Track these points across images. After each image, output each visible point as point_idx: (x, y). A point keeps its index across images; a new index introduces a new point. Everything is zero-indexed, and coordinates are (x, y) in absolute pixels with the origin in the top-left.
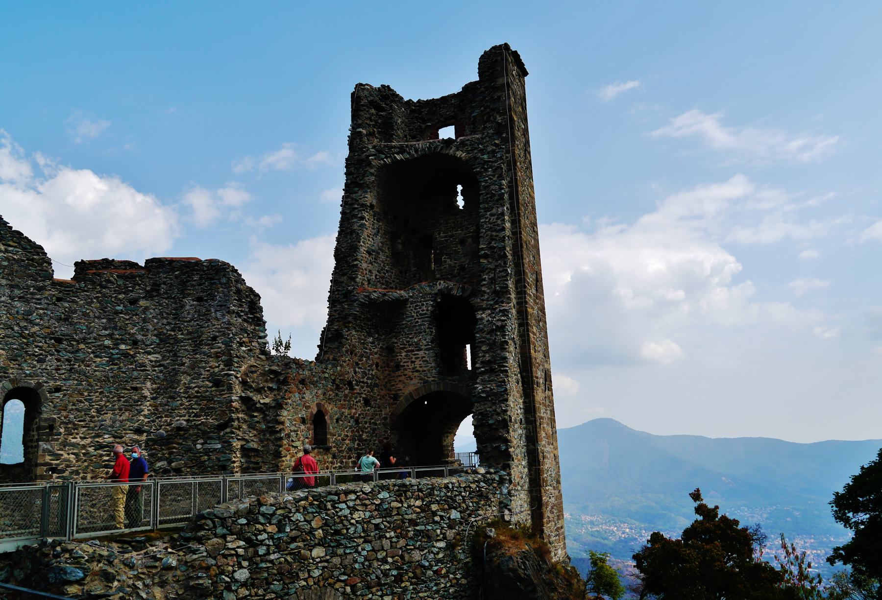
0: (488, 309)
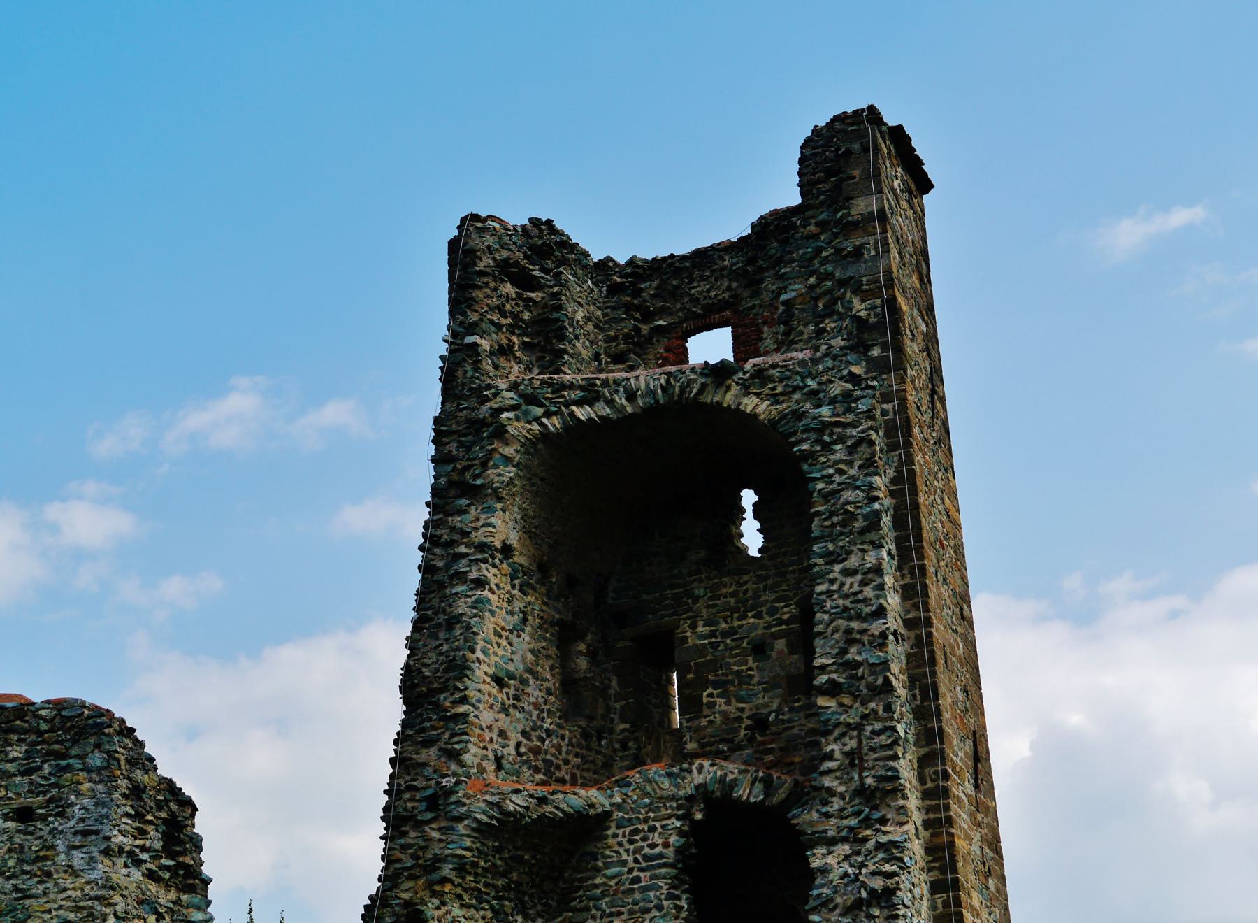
0: (844, 840)
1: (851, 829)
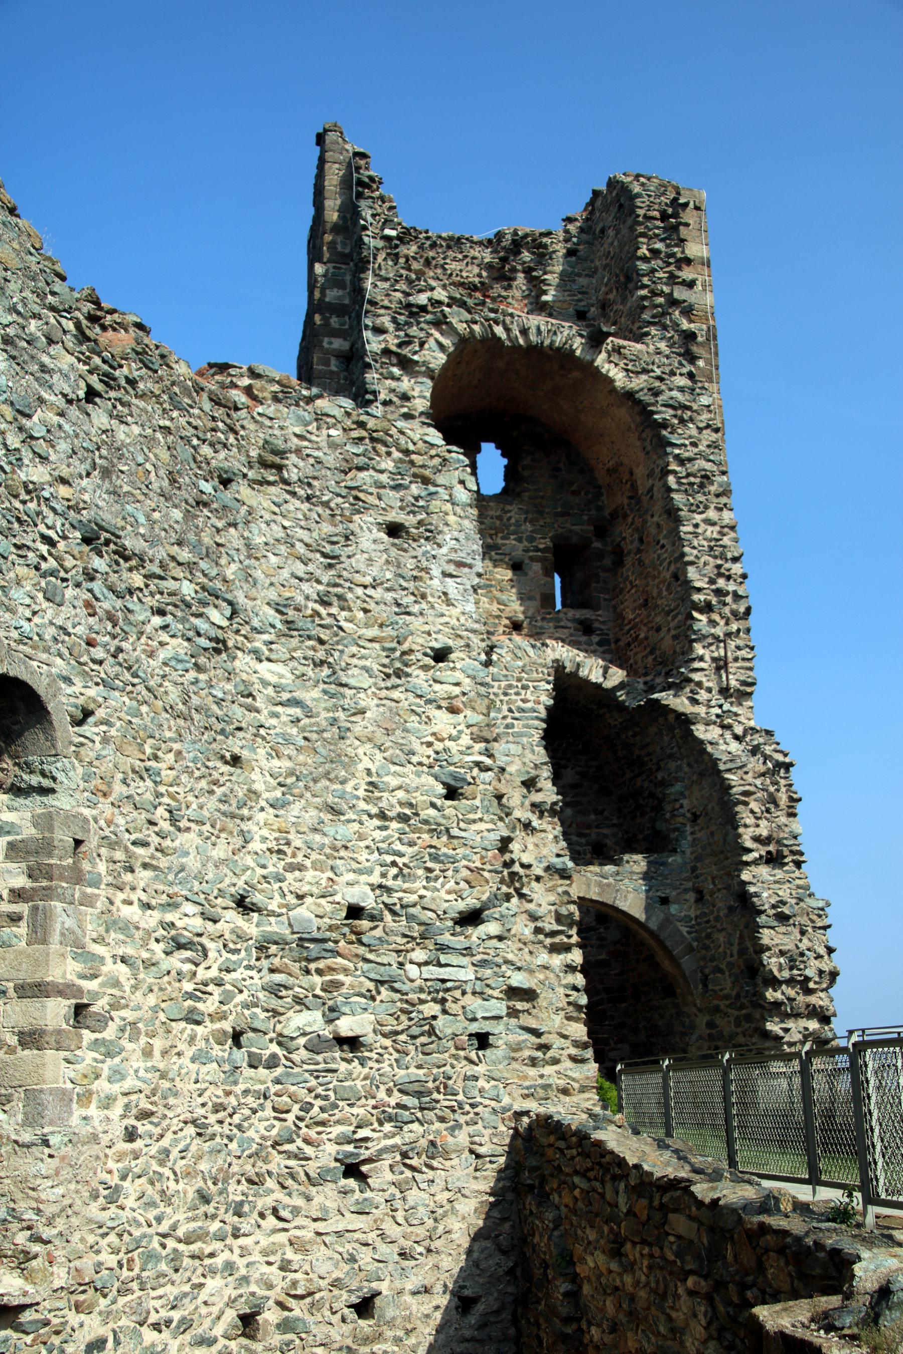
1: (718, 716)
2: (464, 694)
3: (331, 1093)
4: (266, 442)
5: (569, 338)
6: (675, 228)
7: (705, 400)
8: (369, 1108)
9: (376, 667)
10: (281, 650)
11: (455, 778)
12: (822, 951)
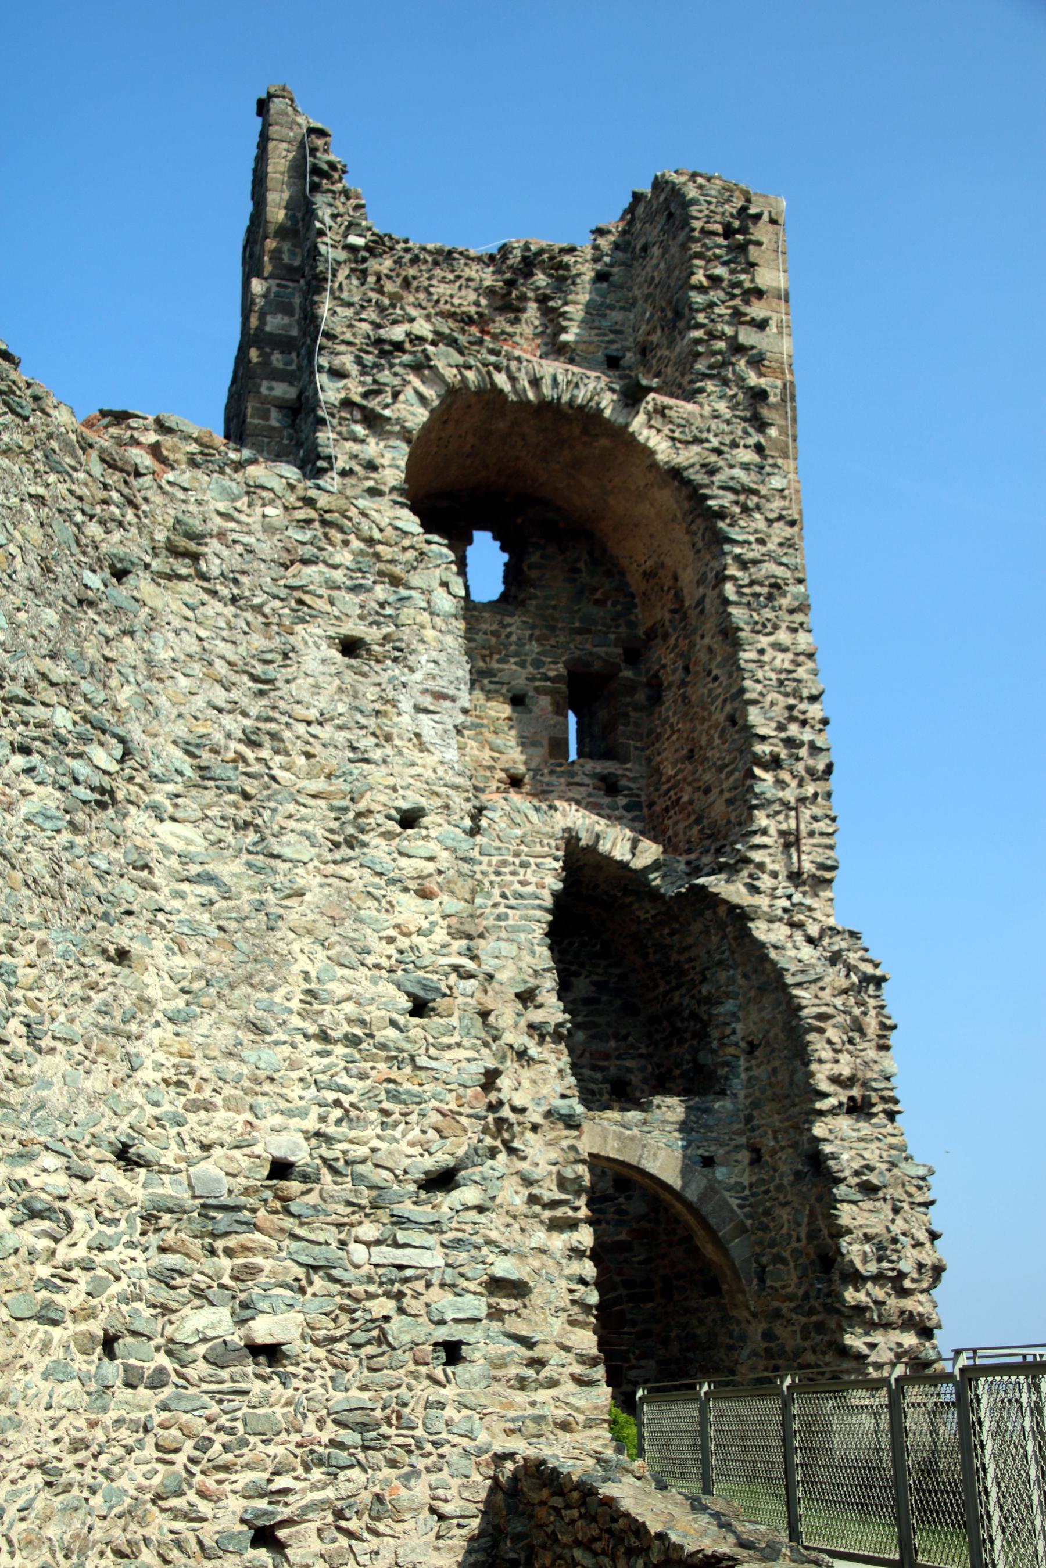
0: (781, 920)
1: (785, 910)
2: (440, 872)
3: (239, 1425)
4: (178, 521)
5: (596, 393)
6: (743, 248)
7: (777, 482)
8: (292, 1447)
9: (320, 833)
10: (190, 806)
11: (425, 988)
12: (923, 1236)
